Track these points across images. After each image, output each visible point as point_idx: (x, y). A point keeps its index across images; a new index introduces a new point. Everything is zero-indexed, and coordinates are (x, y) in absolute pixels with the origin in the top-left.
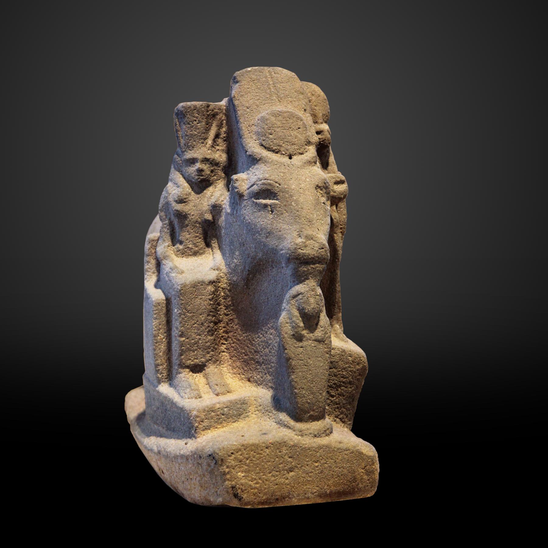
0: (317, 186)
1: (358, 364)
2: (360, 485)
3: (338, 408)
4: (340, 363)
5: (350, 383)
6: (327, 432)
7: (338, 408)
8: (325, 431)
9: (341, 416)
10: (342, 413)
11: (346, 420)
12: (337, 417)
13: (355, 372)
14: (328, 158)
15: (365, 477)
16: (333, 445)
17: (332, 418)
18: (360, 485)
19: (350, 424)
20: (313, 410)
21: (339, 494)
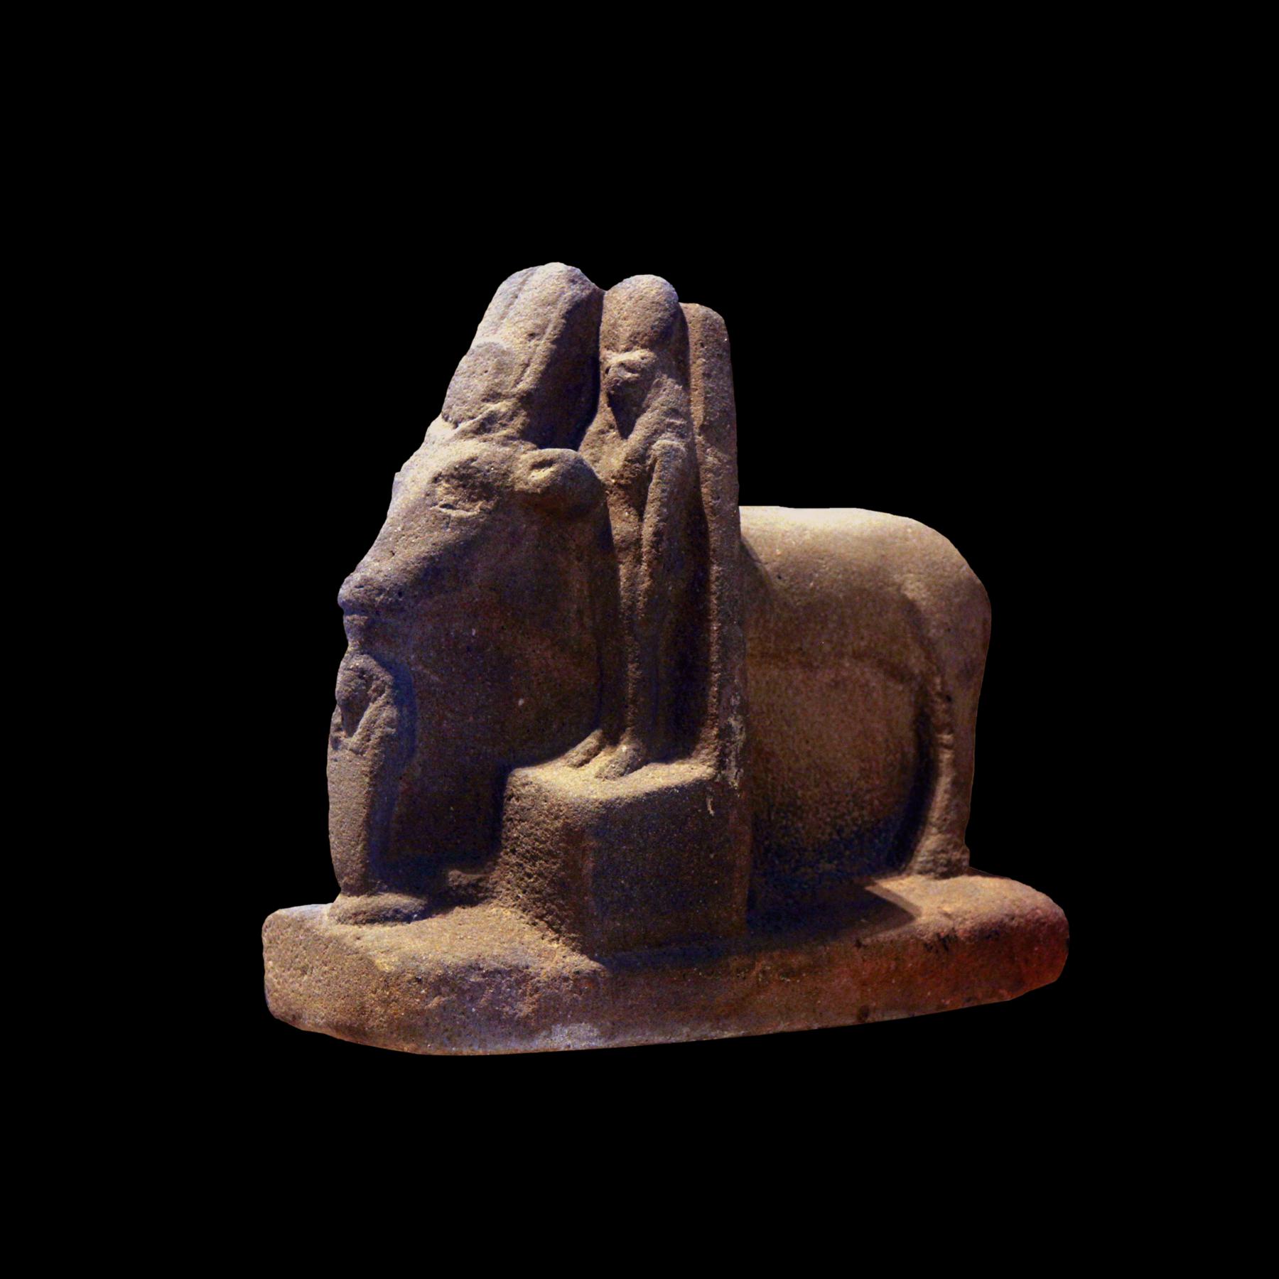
0: (440, 475)
1: (557, 818)
2: (371, 1023)
3: (539, 900)
4: (534, 812)
5: (550, 853)
6: (360, 917)
7: (539, 900)
8: (356, 915)
9: (549, 918)
10: (550, 912)
11: (563, 928)
12: (541, 918)
13: (553, 834)
14: (638, 416)
15: (378, 1009)
16: (348, 940)
17: (527, 918)
18: (371, 1023)
19: (573, 939)
20: (347, 875)
21: (350, 1029)
